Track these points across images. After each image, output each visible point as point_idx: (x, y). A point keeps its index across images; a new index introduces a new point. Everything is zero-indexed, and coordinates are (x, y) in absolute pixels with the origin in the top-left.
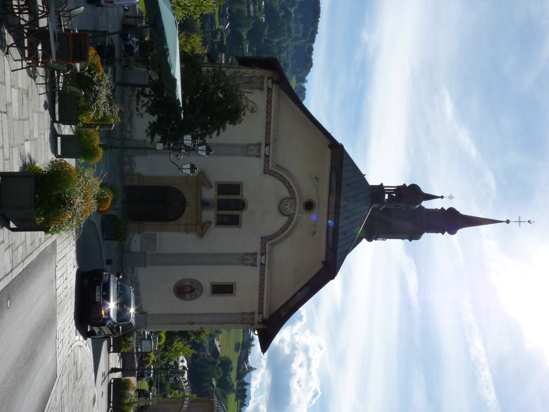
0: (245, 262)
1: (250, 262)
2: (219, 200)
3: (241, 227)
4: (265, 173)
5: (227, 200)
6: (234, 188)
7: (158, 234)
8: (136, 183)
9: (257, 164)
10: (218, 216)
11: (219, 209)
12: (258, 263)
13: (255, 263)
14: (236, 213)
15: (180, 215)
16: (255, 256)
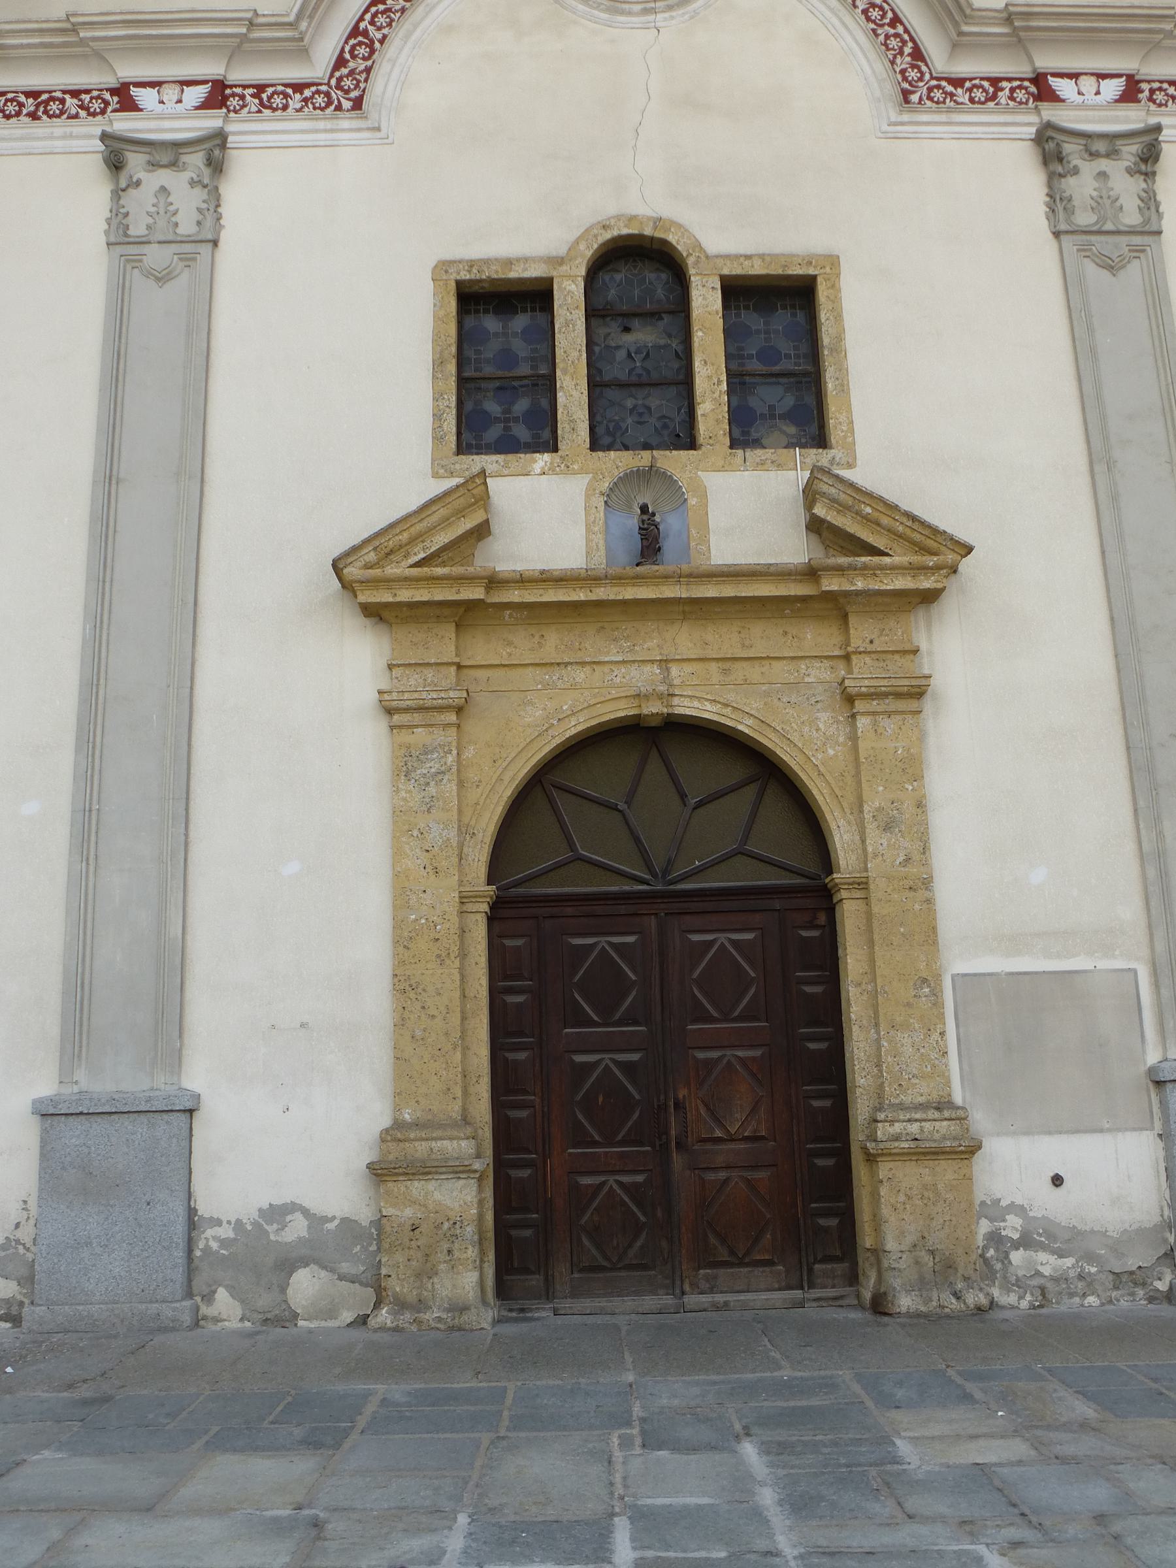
0: (1131, 217)
1: (1126, 188)
2: (601, 438)
3: (833, 261)
4: (358, 104)
5: (596, 385)
6: (492, 311)
7: (959, 961)
8: (463, 1200)
9: (275, 163)
10: (744, 432)
11: (686, 438)
12: (1133, 118)
13: (1130, 150)
14: (706, 301)
15: (764, 772)
16: (1071, 148)
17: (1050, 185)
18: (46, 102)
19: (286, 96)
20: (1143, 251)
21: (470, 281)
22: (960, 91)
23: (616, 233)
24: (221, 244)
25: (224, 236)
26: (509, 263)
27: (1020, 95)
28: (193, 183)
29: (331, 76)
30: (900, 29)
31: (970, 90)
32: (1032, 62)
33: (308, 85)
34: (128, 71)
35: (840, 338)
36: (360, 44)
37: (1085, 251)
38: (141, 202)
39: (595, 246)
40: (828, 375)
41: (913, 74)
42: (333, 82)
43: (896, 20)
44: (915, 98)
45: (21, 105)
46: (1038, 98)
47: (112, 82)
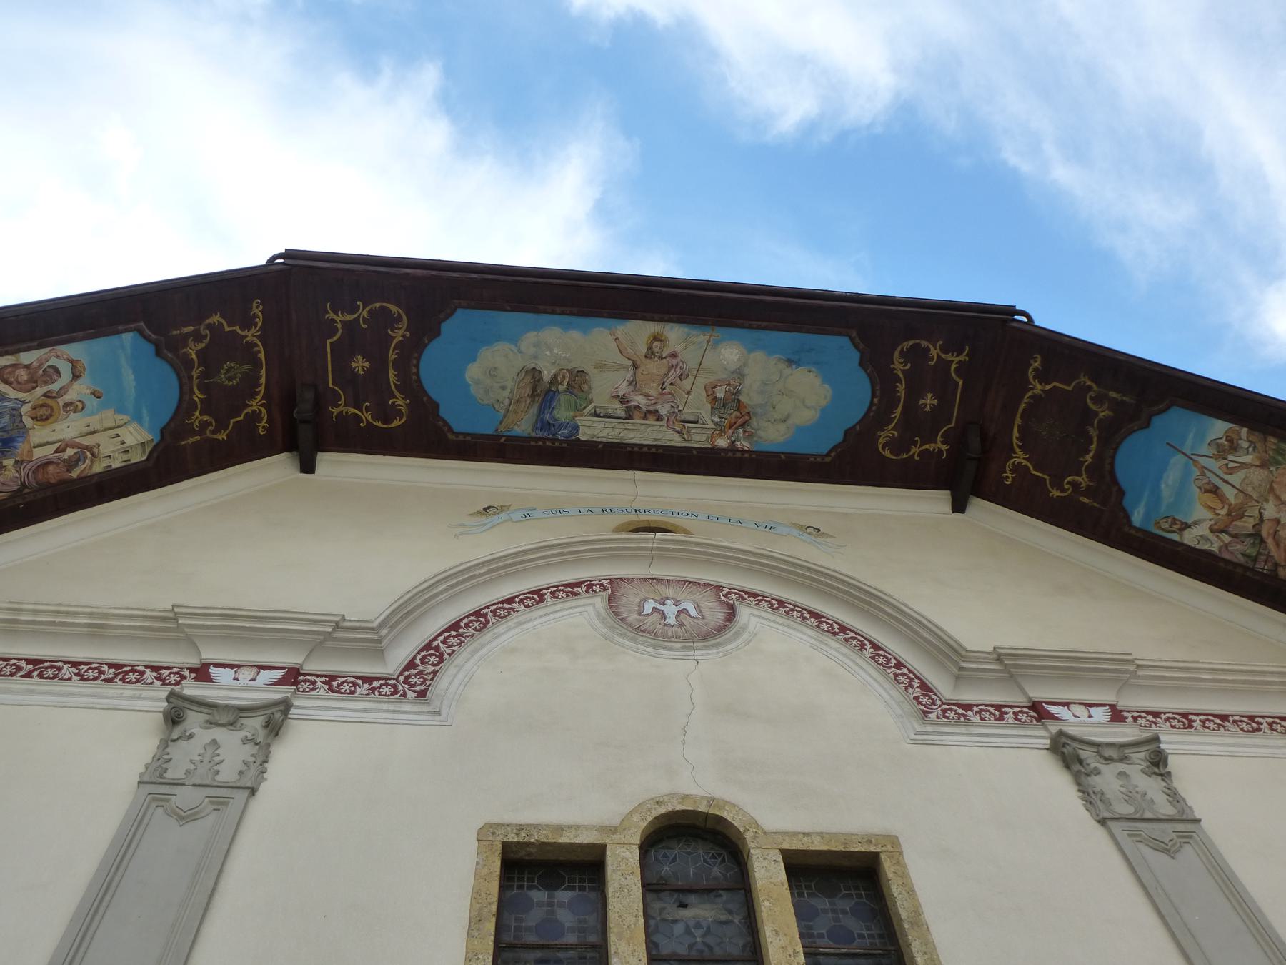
4: (422, 694)
13: (1140, 756)
14: (768, 875)
17: (1078, 784)
18: (127, 673)
19: (355, 685)
20: (1190, 837)
21: (518, 843)
22: (970, 713)
23: (670, 809)
24: (259, 794)
25: (264, 789)
26: (560, 829)
27: (1023, 717)
28: (245, 741)
29: (401, 674)
30: (905, 671)
31: (979, 712)
32: (1025, 693)
33: (378, 679)
34: (209, 655)
35: (917, 911)
36: (431, 655)
37: (1133, 834)
38: (184, 756)
39: (650, 819)
40: (914, 950)
41: (925, 700)
42: (402, 678)
43: (899, 665)
44: (933, 716)
45: (101, 672)
46: (1039, 719)
47: (195, 662)
